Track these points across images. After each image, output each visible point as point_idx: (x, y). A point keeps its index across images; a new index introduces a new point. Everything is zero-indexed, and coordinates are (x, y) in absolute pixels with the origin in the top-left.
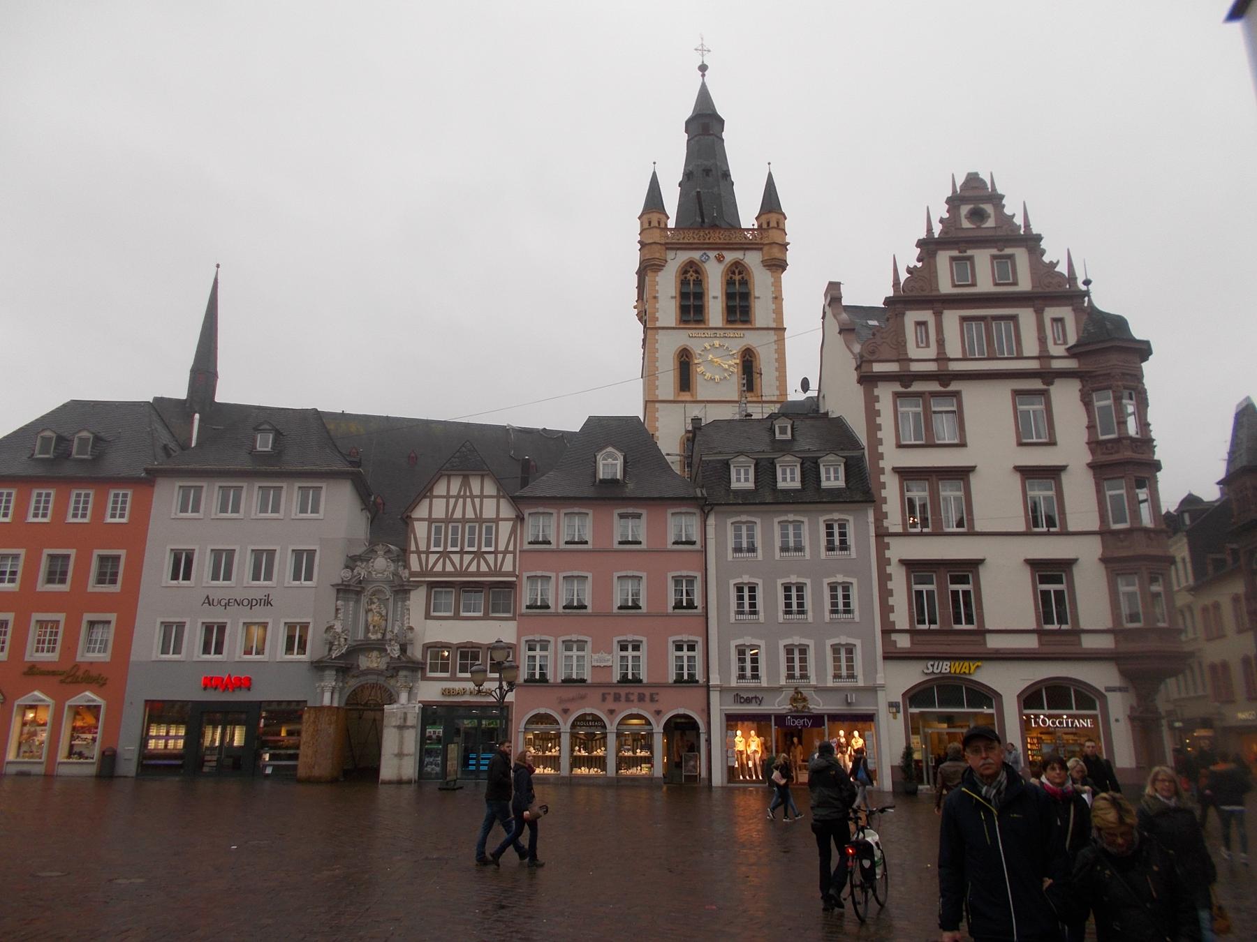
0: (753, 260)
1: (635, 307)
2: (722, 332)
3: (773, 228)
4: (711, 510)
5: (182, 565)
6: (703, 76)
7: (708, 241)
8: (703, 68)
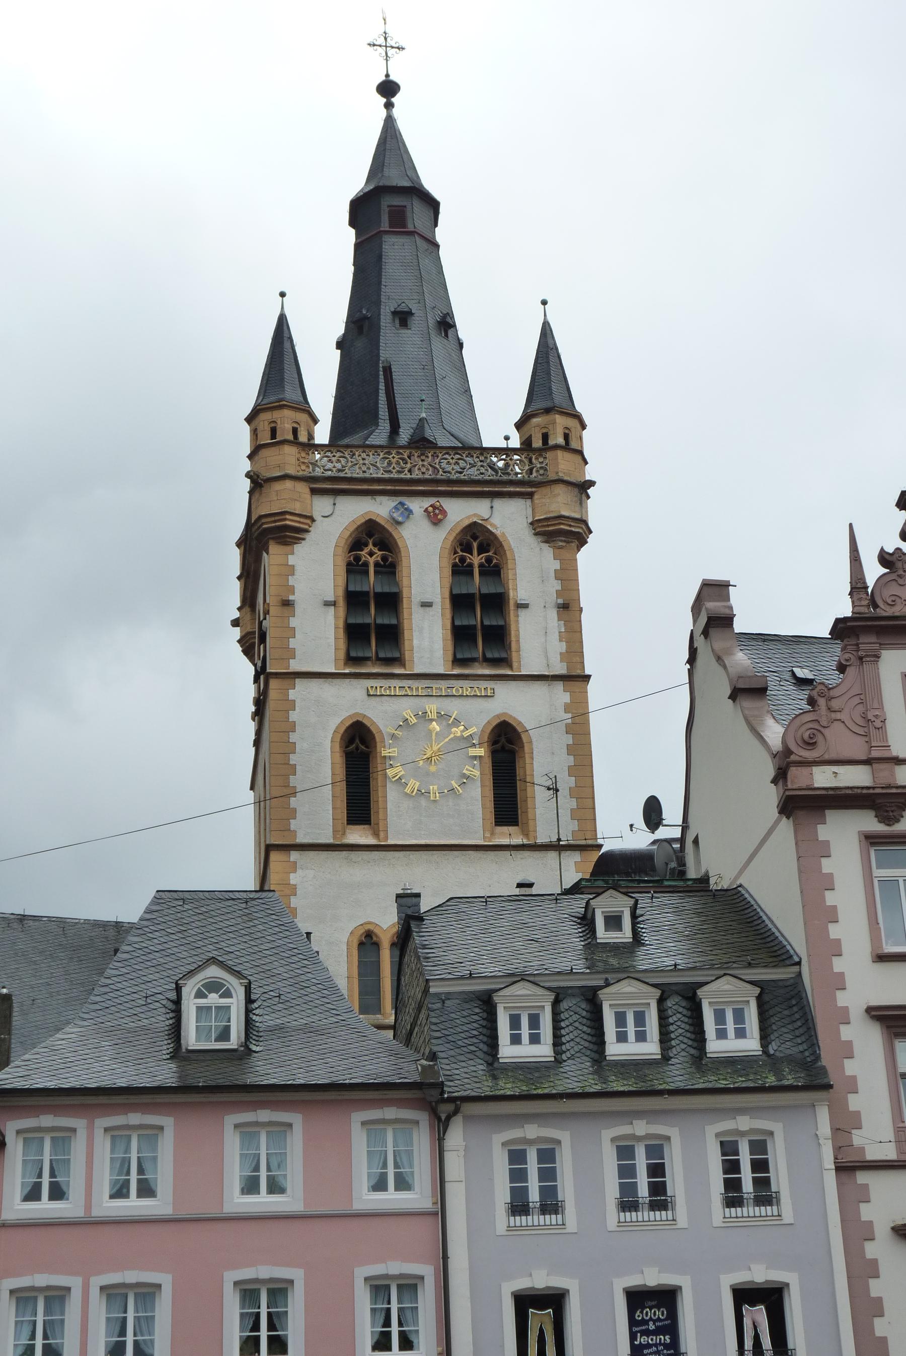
1: (235, 623)
2: (443, 684)
3: (557, 447)
4: (456, 1112)
6: (389, 106)
7: (409, 476)
8: (388, 89)
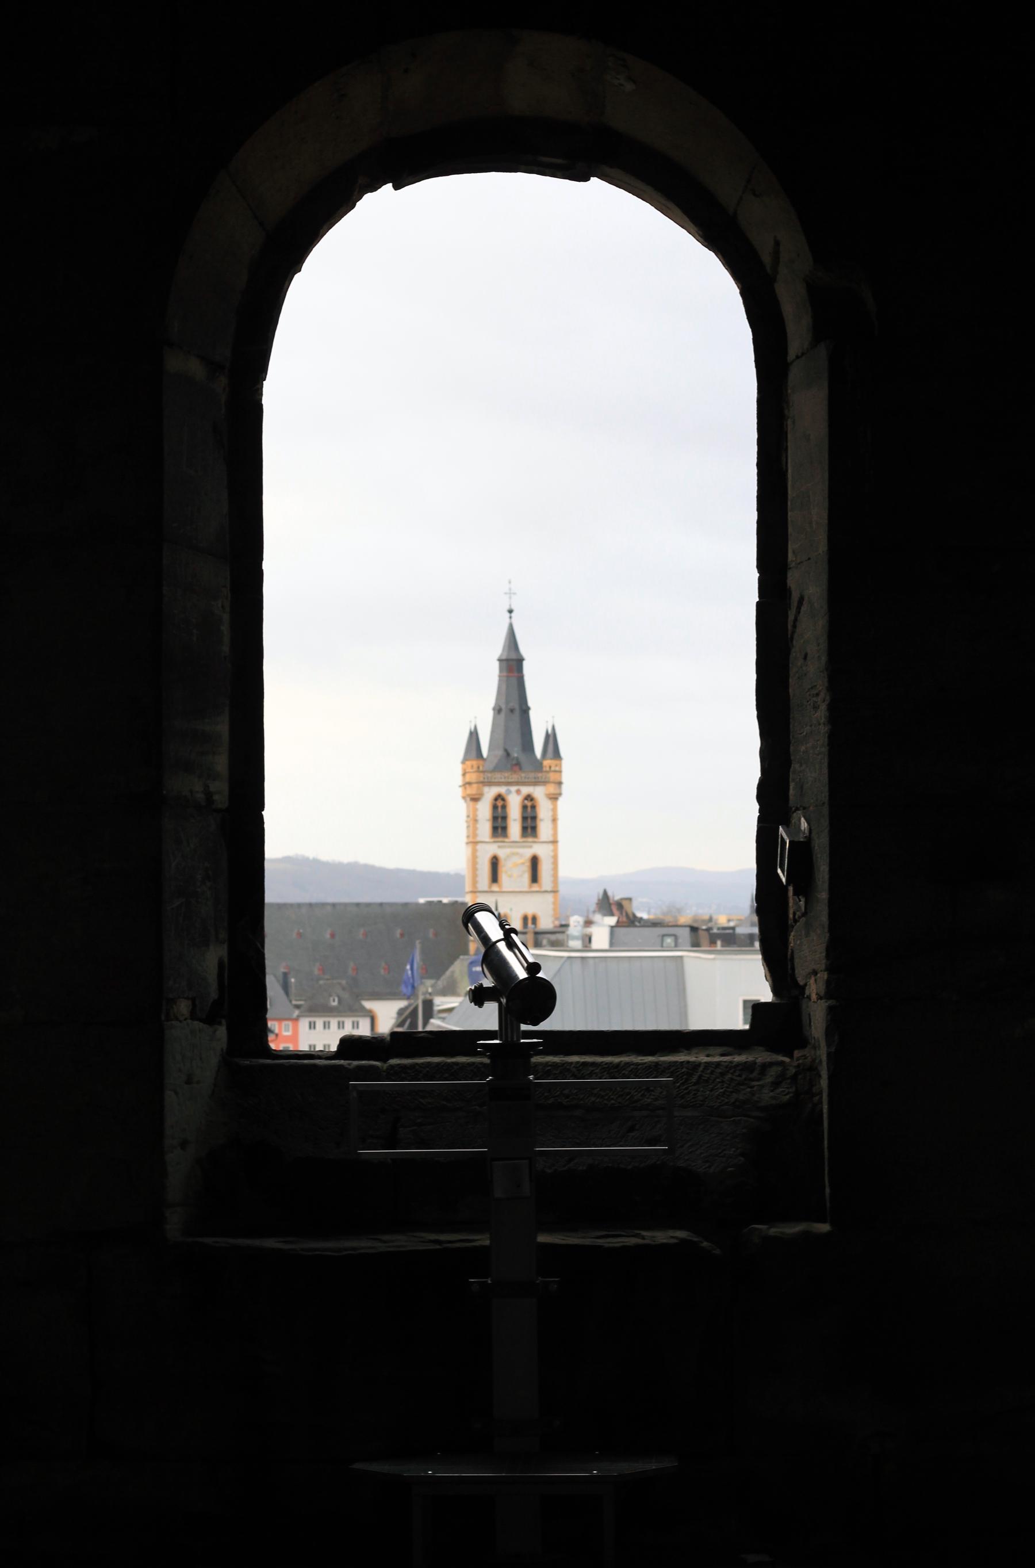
0: (539, 792)
6: (511, 617)
8: (510, 611)
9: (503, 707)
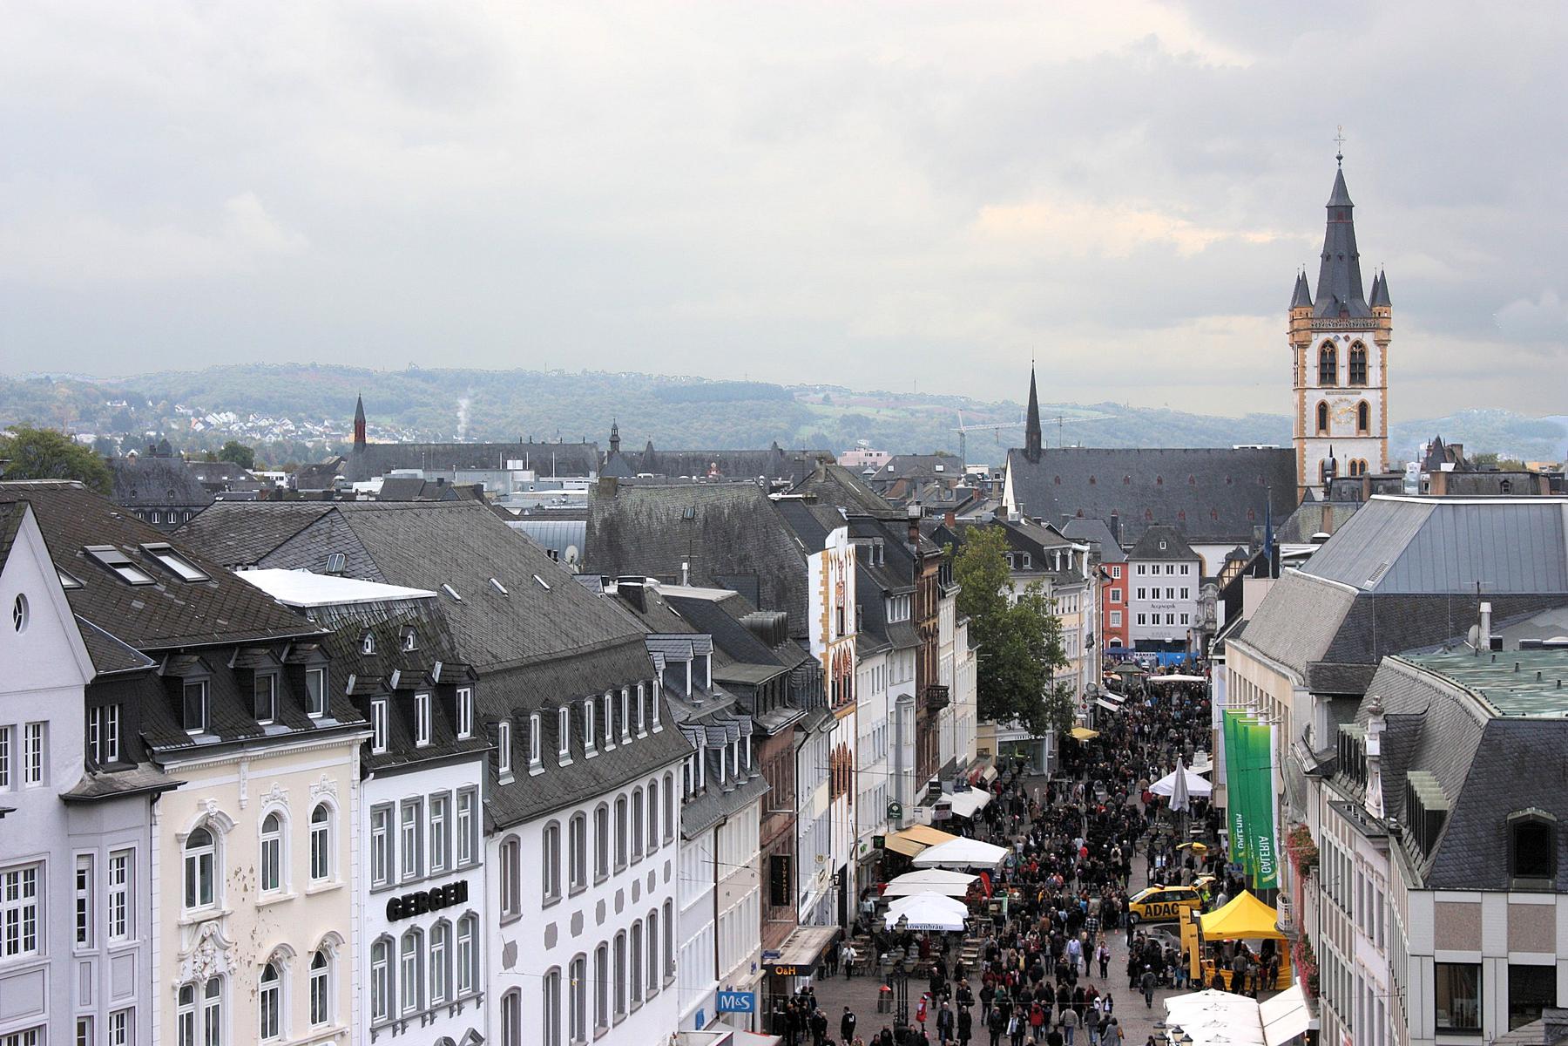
0: (1368, 339)
5: (1142, 593)
6: (1340, 164)
8: (1340, 158)
9: (1331, 253)
